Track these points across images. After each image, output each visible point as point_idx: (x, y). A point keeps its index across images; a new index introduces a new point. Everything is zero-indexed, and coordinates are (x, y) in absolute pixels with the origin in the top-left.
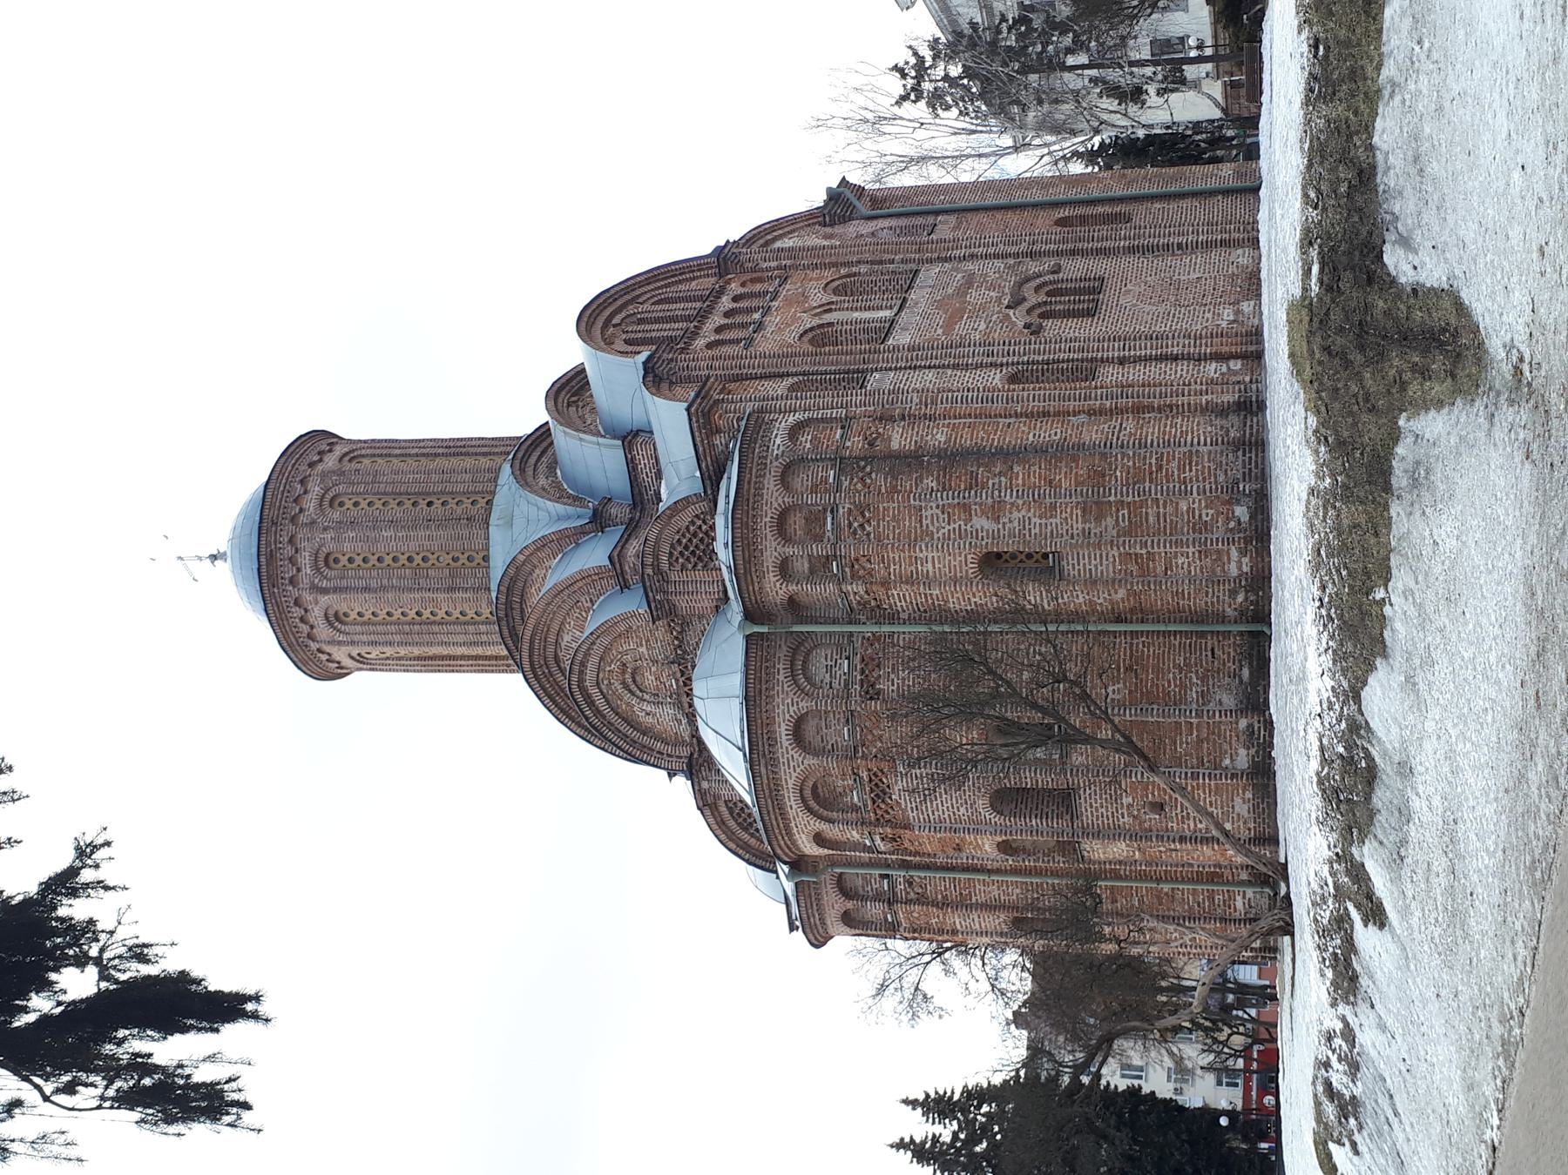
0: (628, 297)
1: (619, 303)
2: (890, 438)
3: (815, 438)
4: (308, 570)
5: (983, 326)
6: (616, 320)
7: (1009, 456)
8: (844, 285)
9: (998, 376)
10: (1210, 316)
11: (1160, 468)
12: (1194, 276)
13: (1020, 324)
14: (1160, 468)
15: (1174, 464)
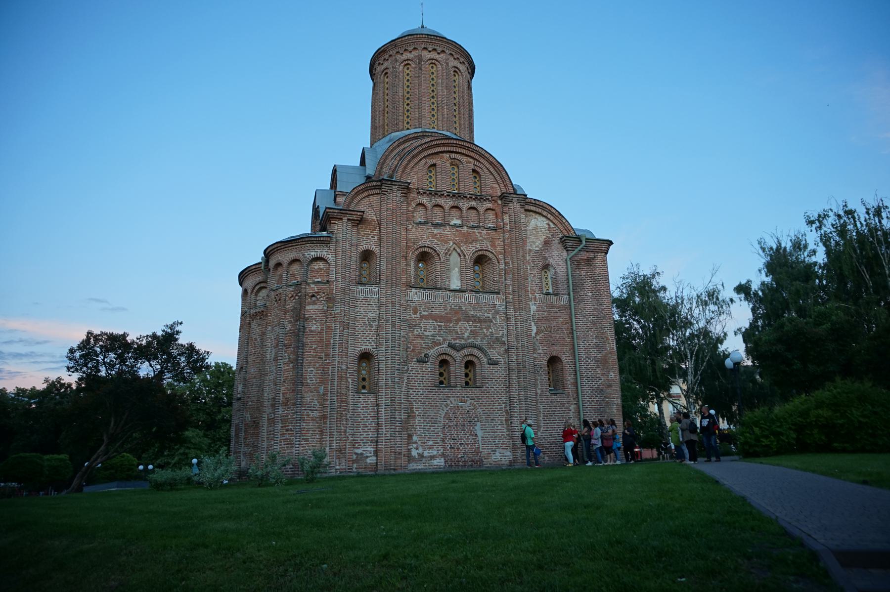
0: (477, 157)
1: (472, 154)
2: (314, 303)
3: (321, 269)
4: (383, 67)
5: (426, 333)
6: (453, 156)
7: (297, 363)
8: (490, 259)
9: (370, 347)
10: (431, 443)
11: (287, 430)
12: (480, 433)
13: (431, 352)
14: (287, 430)
15: (288, 437)
